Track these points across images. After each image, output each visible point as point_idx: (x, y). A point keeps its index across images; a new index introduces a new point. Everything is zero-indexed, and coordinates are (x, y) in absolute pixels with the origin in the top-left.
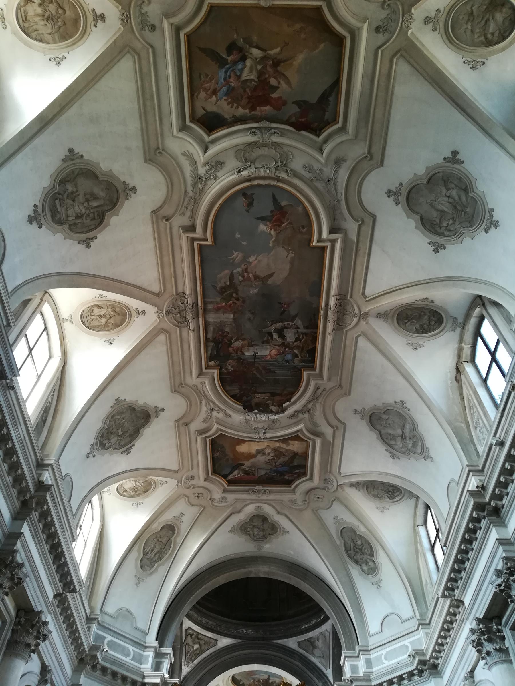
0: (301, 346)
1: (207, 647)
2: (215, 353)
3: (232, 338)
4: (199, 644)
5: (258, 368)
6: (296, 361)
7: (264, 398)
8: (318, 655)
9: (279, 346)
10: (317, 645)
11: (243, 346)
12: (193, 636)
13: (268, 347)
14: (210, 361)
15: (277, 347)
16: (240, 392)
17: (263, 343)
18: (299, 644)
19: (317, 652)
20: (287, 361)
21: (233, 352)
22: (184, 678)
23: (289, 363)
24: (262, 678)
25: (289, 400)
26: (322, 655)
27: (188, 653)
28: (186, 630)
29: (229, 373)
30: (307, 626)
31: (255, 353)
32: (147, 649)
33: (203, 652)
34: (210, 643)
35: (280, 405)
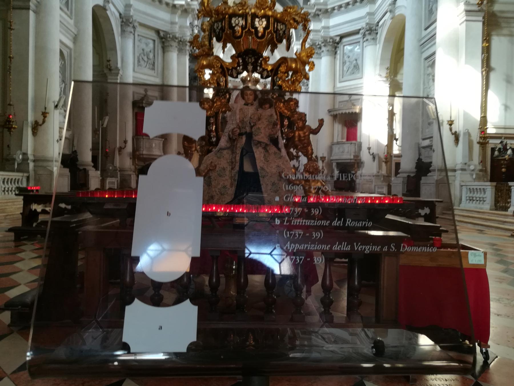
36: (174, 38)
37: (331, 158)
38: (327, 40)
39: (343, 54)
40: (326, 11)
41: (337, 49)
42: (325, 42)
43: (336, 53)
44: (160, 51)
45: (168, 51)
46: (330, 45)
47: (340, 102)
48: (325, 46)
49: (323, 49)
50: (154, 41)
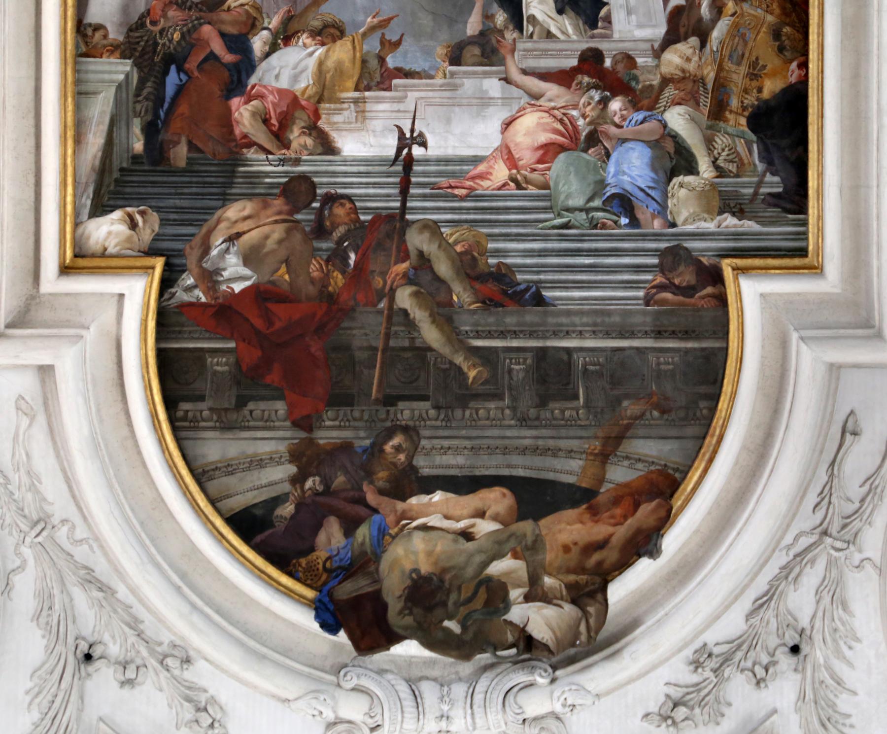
0: (710, 74)
2: (138, 146)
3: (253, 25)
5: (424, 261)
6: (684, 196)
7: (467, 535)
9: (564, 78)
11: (325, 90)
13: (493, 86)
14: (100, 209)
15: (552, 89)
16: (297, 480)
17: (456, 59)
20: (623, 203)
21: (261, 136)
23: (634, 222)
25: (645, 543)
29: (224, 313)
31: (404, 142)
35: (587, 591)
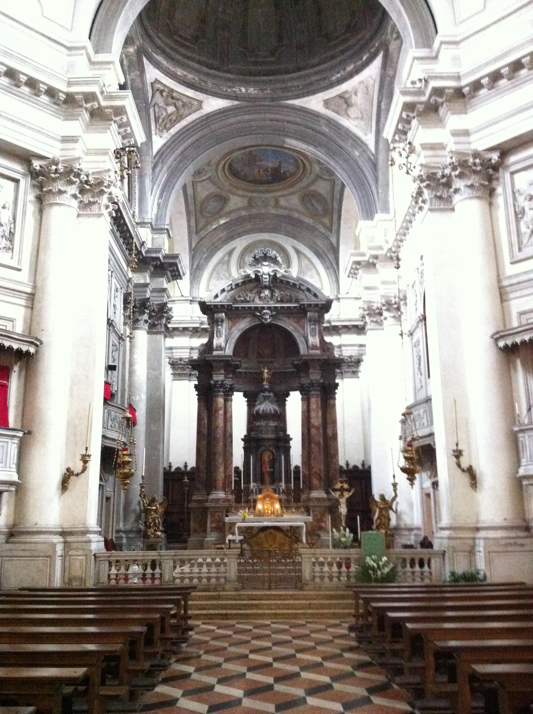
1: (187, 112)
4: (175, 106)
8: (355, 116)
10: (353, 102)
12: (164, 94)
18: (327, 103)
19: (352, 112)
22: (158, 153)
24: (270, 165)
26: (360, 116)
27: (159, 118)
28: (152, 84)
30: (339, 75)
32: (73, 52)
33: (180, 118)
34: (192, 105)
36: (70, 173)
37: (522, 472)
38: (466, 161)
39: (514, 193)
40: (459, 93)
41: (495, 183)
42: (463, 166)
43: (492, 192)
44: (31, 208)
45: (51, 205)
46: (475, 172)
47: (521, 314)
48: (461, 176)
49: (458, 184)
50: (17, 181)
